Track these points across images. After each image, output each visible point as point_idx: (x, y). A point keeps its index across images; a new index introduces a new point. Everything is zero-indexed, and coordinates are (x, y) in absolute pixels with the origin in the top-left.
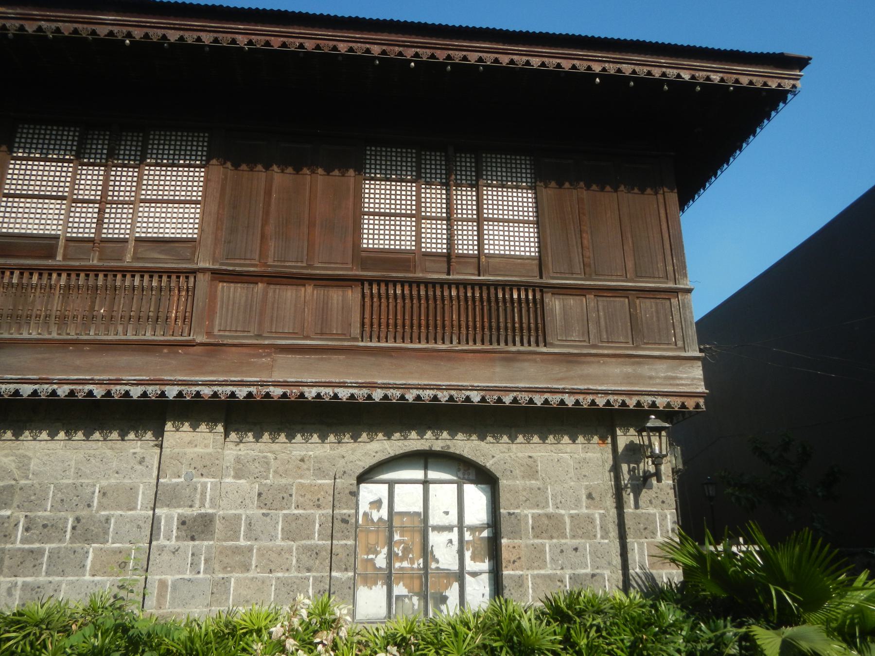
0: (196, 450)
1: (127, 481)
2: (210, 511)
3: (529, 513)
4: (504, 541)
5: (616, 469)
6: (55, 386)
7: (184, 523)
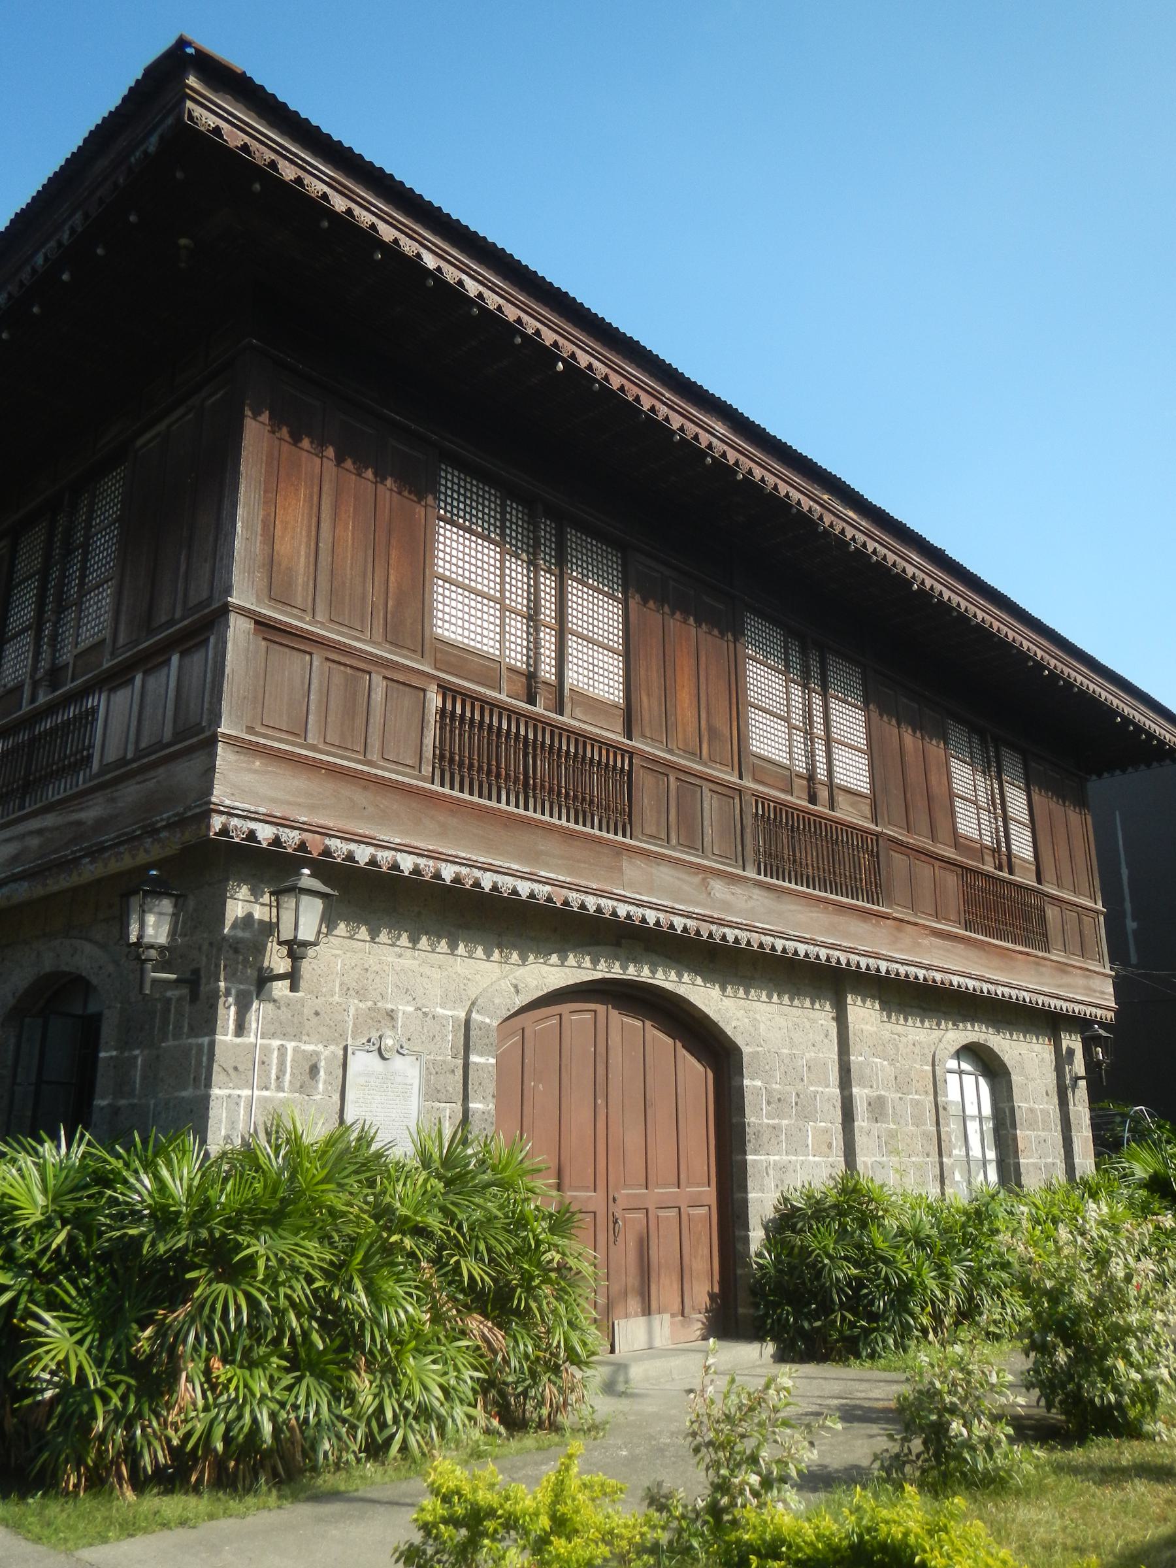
0: (868, 1027)
1: (821, 1055)
2: (883, 1093)
3: (1024, 1105)
4: (1018, 1132)
5: (1059, 1070)
6: (817, 948)
7: (870, 1104)
